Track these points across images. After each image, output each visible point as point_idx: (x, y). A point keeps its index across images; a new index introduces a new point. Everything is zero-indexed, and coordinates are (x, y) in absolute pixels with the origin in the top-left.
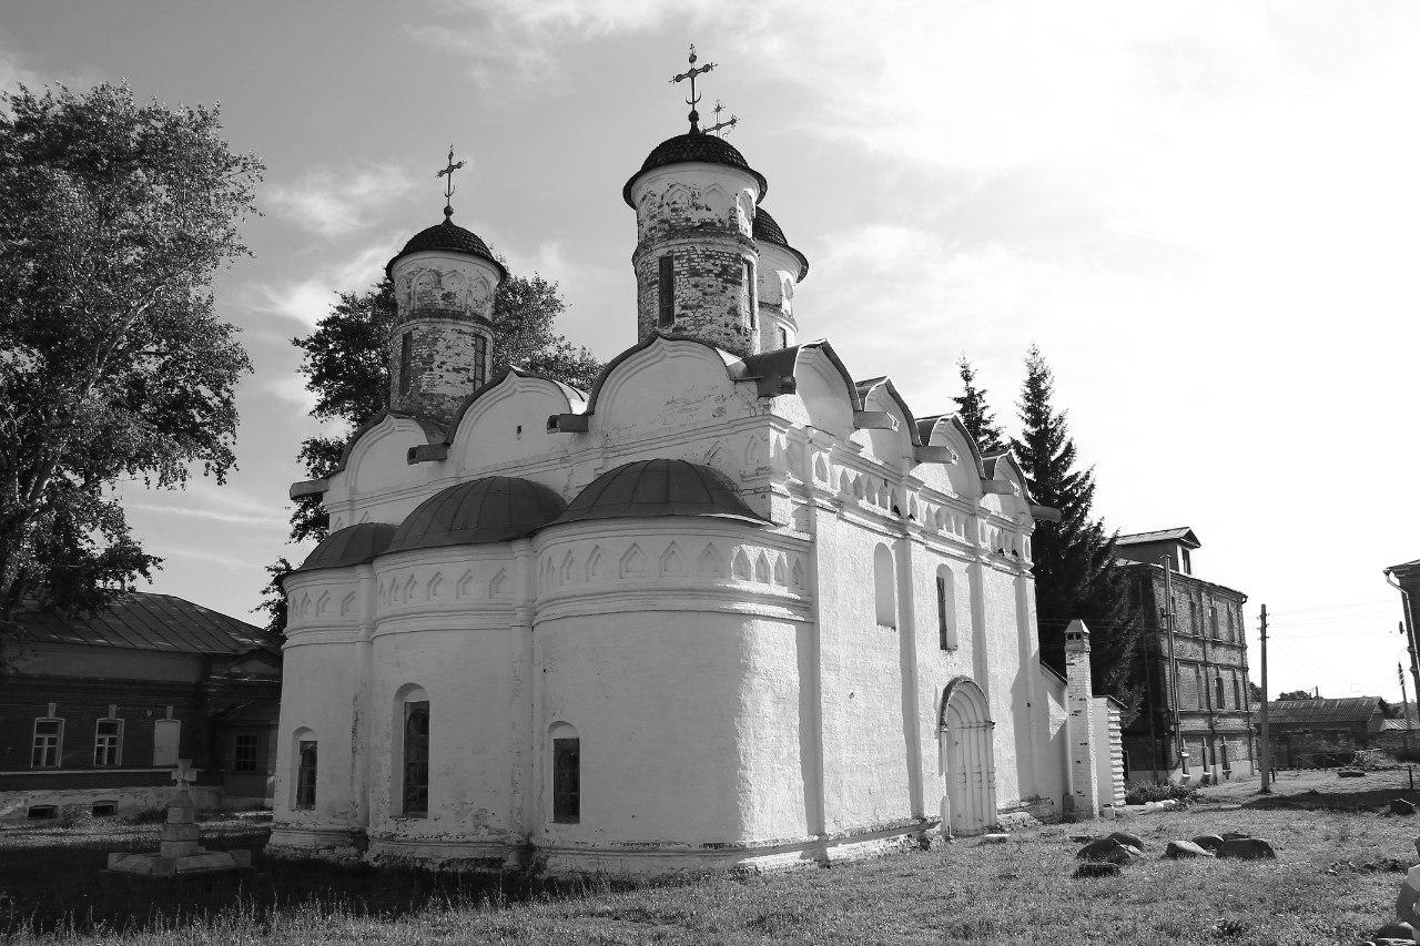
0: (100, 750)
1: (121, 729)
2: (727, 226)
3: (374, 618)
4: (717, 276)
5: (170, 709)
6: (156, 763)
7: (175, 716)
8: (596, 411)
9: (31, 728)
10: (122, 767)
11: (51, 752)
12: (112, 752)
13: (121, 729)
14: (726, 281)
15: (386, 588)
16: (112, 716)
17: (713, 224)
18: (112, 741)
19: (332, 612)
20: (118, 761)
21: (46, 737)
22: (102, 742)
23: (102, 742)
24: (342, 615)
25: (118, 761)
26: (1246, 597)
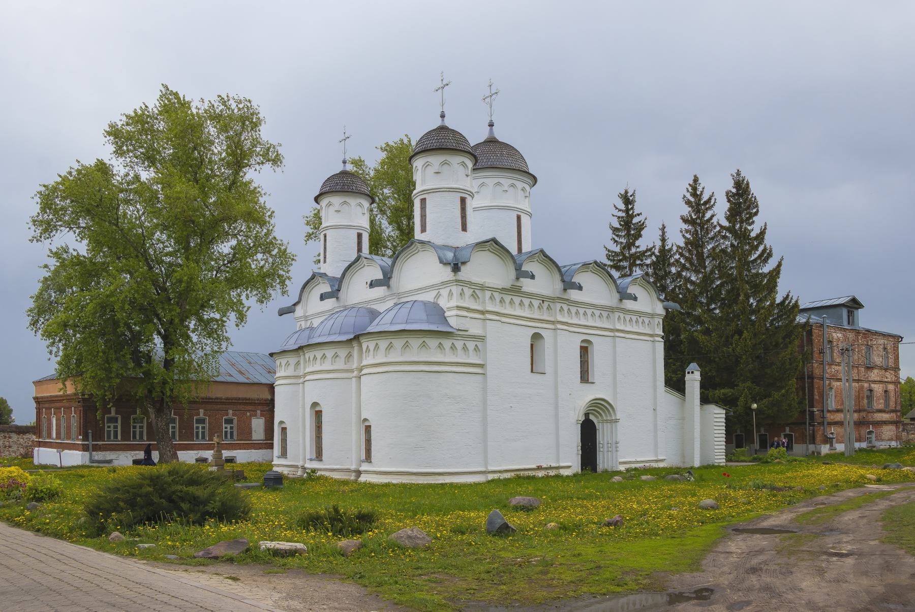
0: (226, 432)
1: (235, 422)
5: (259, 412)
6: (254, 438)
7: (262, 415)
8: (393, 276)
9: (193, 421)
11: (203, 433)
12: (232, 433)
15: (311, 359)
18: (231, 428)
19: (290, 372)
20: (235, 437)
21: (200, 426)
22: (226, 427)
23: (226, 427)
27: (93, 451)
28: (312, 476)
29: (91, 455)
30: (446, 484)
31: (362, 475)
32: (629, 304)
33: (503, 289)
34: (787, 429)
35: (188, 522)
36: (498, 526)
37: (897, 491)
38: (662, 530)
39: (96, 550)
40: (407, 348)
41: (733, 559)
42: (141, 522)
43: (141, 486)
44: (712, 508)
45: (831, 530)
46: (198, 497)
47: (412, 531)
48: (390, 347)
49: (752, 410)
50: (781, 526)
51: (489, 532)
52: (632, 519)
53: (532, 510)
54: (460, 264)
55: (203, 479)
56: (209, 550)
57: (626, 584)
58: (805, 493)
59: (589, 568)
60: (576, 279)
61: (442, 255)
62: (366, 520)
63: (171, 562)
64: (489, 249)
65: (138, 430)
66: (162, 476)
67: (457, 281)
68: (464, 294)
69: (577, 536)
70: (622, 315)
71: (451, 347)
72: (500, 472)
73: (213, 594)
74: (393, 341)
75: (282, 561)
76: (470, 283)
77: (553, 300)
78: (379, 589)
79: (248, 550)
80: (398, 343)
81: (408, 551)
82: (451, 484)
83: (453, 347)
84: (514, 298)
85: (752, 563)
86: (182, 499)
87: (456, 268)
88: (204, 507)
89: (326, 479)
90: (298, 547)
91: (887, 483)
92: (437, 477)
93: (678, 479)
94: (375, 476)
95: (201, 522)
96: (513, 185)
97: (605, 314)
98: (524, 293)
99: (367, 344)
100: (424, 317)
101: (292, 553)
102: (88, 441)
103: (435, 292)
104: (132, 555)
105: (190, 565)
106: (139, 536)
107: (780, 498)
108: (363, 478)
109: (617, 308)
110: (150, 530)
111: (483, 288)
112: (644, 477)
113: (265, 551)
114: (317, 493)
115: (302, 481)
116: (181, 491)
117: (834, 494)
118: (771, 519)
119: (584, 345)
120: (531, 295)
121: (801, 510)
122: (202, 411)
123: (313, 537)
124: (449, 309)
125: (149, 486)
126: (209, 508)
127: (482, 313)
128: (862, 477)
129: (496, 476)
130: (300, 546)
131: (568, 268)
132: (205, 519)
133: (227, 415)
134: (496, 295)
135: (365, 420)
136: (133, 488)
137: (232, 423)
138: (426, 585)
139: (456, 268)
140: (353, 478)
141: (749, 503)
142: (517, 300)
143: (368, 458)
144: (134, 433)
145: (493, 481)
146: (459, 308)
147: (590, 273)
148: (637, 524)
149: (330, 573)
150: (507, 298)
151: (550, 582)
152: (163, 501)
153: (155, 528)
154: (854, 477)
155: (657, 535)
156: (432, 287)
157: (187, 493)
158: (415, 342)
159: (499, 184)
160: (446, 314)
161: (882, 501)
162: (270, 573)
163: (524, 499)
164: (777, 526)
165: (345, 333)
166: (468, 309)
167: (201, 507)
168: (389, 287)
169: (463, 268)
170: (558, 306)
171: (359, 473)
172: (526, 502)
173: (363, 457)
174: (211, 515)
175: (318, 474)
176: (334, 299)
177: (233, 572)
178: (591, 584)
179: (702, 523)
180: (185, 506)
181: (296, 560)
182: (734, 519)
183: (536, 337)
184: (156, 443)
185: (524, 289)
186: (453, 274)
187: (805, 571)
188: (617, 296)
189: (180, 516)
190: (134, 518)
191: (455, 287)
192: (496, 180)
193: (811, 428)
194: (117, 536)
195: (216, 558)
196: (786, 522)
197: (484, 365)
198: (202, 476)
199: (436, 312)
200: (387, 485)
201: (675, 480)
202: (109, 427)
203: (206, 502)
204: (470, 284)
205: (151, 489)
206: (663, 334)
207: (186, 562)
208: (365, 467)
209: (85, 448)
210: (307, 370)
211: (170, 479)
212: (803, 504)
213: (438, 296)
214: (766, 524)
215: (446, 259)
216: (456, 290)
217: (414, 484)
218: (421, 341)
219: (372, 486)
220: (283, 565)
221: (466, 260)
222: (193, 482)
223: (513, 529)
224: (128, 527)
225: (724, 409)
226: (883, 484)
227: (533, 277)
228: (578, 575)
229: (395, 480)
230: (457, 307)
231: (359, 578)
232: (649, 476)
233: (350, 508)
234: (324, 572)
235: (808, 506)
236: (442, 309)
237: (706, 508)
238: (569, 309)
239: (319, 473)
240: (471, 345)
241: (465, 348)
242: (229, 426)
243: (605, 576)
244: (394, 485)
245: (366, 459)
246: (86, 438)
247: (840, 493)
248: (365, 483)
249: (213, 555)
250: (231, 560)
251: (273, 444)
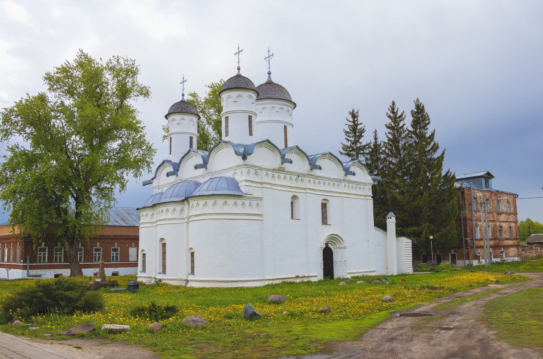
0: (113, 257)
1: (119, 250)
3: (189, 215)
6: (130, 260)
10: (120, 262)
12: (117, 257)
13: (119, 250)
15: (160, 212)
16: (116, 246)
18: (117, 254)
19: (148, 219)
20: (119, 260)
21: (97, 253)
22: (114, 254)
23: (114, 254)
24: (151, 219)
25: (119, 260)
26: (518, 196)
27: (29, 269)
28: (159, 284)
29: (28, 271)
30: (238, 287)
31: (189, 283)
32: (350, 178)
33: (274, 170)
34: (453, 251)
35: (64, 313)
36: (250, 314)
37: (506, 288)
38: (352, 315)
39: (3, 332)
41: (384, 333)
42: (35, 314)
43: (36, 291)
44: (390, 301)
45: (454, 314)
46: (71, 298)
47: (196, 317)
48: (205, 204)
49: (430, 240)
50: (425, 311)
51: (245, 317)
52: (338, 309)
53: (281, 303)
54: (247, 155)
55: (76, 287)
56: (70, 330)
57: (309, 349)
58: (450, 291)
59: (291, 339)
60: (318, 163)
61: (236, 150)
62: (171, 310)
63: (45, 338)
65: (58, 256)
66: (51, 285)
67: (245, 165)
69: (298, 319)
70: (347, 184)
71: (242, 204)
72: (273, 280)
73: (59, 357)
74: (207, 201)
75: (113, 336)
77: (304, 175)
78: (162, 353)
79: (94, 330)
80: (210, 202)
81: (191, 329)
82: (241, 288)
84: (280, 174)
85: (394, 335)
86: (62, 299)
87: (244, 158)
88: (75, 304)
89: (166, 285)
90: (125, 328)
91: (503, 283)
92: (234, 283)
93: (378, 283)
94: (196, 283)
95: (71, 313)
96: (281, 108)
97: (336, 183)
98: (287, 171)
99: (193, 202)
100: (226, 186)
101: (120, 331)
102: (26, 263)
104: (23, 334)
105: (57, 340)
106: (32, 322)
107: (433, 294)
108: (189, 285)
109: (344, 180)
110: (40, 318)
111: (261, 169)
112: (358, 282)
113: (104, 330)
114: (158, 294)
115: (153, 286)
116: (61, 294)
117: (468, 291)
118: (423, 307)
119: (324, 202)
120: (291, 173)
121: (443, 301)
122: (98, 244)
123: (136, 321)
124: (241, 181)
125: (41, 291)
126: (78, 304)
127: (261, 183)
128: (488, 280)
129: (270, 282)
130: (126, 327)
131: (313, 157)
132: (74, 312)
133: (114, 246)
134: (269, 173)
135: (191, 249)
136: (32, 293)
137: (100, 251)
138: (191, 350)
139: (244, 158)
140: (184, 284)
141: (413, 298)
142: (282, 176)
143: (193, 272)
144: (56, 258)
145: (268, 285)
146: (246, 181)
147: (327, 160)
148: (339, 312)
149: (139, 343)
150: (276, 175)
151: (265, 348)
152: (49, 300)
153: (43, 318)
154: (482, 280)
155: (349, 318)
157: (65, 296)
158: (220, 201)
160: (239, 185)
161: (494, 295)
162: (103, 344)
163: (276, 297)
164: (423, 312)
165: (180, 196)
166: (252, 182)
167: (72, 304)
168: (206, 168)
169: (249, 157)
170: (308, 179)
171: (187, 281)
172: (277, 298)
173: (190, 272)
174: (78, 308)
175: (162, 282)
176: (175, 176)
177: (80, 343)
178: (288, 349)
179: (380, 310)
180: (62, 303)
181: (122, 336)
182: (400, 308)
183: (294, 197)
184: (69, 264)
185: (286, 169)
186: (243, 161)
187: (421, 339)
188: (343, 173)
189: (59, 309)
190: (31, 311)
191: (244, 168)
193: (466, 250)
194: (17, 323)
195: (74, 335)
196: (430, 309)
198: (75, 285)
199: (234, 183)
200: (202, 289)
201: (376, 283)
202: (40, 254)
203: (76, 301)
205: (42, 294)
206: (372, 195)
207: (54, 337)
208: (191, 278)
209: (24, 268)
210: (158, 219)
211: (55, 287)
212: (447, 297)
213: (235, 173)
214: (417, 311)
215: (239, 152)
216: (245, 170)
217: (218, 288)
218: (224, 201)
219: (193, 289)
220: (113, 339)
221: (251, 153)
222: (69, 288)
223: (260, 315)
224: (27, 317)
225: (411, 239)
226: (499, 284)
227: (291, 162)
228: (284, 343)
229: (208, 285)
230: (246, 180)
231: (155, 346)
232: (362, 282)
233: (162, 302)
234: (135, 343)
235: (449, 299)
236: (237, 182)
237: (385, 301)
238: (314, 181)
239: (163, 282)
240: (254, 203)
241: (250, 205)
242: (115, 253)
243: (299, 344)
244: (206, 289)
245: (192, 272)
246: (25, 261)
247: (472, 290)
248: (189, 288)
249: (72, 333)
250: (82, 336)
251: (138, 263)
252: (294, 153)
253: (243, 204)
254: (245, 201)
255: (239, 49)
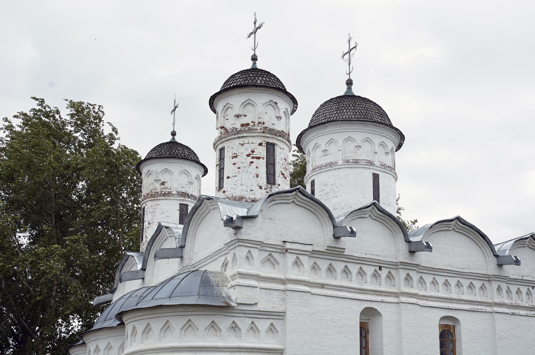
2: (256, 124)
4: (248, 155)
14: (253, 158)
17: (248, 125)
32: (510, 270)
33: (314, 253)
40: (190, 329)
64: (293, 202)
68: (253, 258)
76: (261, 244)
83: (235, 327)
84: (334, 264)
96: (367, 140)
97: (478, 284)
103: (223, 259)
119: (446, 322)
120: (361, 261)
127: (283, 282)
142: (339, 266)
147: (453, 233)
150: (323, 264)
156: (218, 253)
159: (350, 139)
168: (182, 257)
170: (403, 274)
188: (494, 260)
192: (346, 135)
197: (283, 350)
204: (260, 245)
240: (263, 325)
252: (369, 218)
253: (235, 327)
254: (237, 321)
255: (255, 23)
